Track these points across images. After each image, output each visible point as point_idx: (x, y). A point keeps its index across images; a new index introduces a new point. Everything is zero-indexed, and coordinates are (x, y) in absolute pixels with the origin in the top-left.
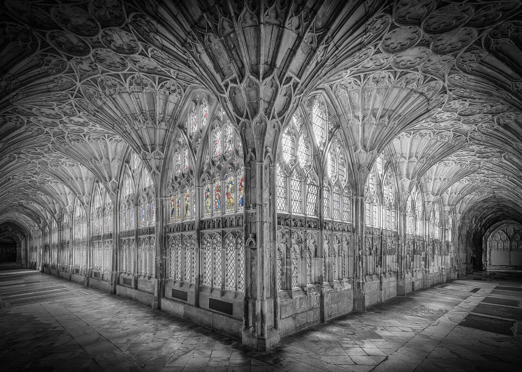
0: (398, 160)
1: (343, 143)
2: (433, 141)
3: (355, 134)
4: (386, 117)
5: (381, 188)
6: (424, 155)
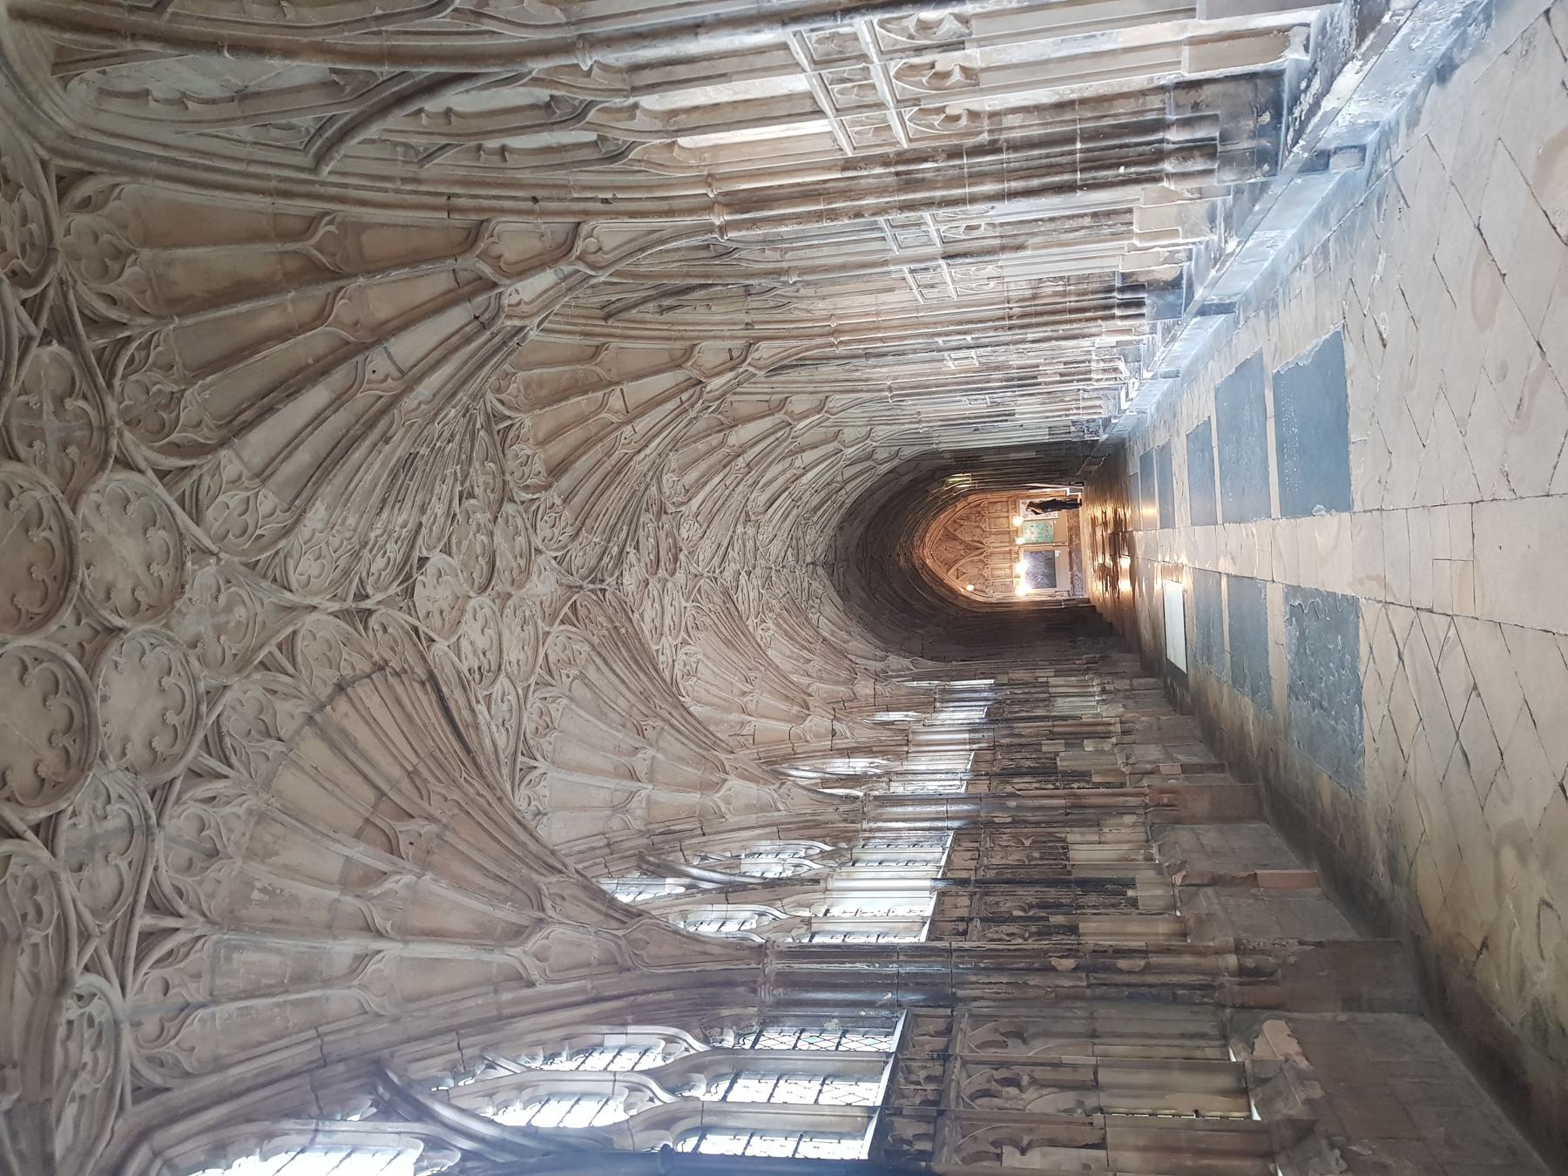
0: (638, 825)
2: (579, 689)
3: (439, 981)
4: (401, 826)
5: (744, 887)
6: (629, 725)
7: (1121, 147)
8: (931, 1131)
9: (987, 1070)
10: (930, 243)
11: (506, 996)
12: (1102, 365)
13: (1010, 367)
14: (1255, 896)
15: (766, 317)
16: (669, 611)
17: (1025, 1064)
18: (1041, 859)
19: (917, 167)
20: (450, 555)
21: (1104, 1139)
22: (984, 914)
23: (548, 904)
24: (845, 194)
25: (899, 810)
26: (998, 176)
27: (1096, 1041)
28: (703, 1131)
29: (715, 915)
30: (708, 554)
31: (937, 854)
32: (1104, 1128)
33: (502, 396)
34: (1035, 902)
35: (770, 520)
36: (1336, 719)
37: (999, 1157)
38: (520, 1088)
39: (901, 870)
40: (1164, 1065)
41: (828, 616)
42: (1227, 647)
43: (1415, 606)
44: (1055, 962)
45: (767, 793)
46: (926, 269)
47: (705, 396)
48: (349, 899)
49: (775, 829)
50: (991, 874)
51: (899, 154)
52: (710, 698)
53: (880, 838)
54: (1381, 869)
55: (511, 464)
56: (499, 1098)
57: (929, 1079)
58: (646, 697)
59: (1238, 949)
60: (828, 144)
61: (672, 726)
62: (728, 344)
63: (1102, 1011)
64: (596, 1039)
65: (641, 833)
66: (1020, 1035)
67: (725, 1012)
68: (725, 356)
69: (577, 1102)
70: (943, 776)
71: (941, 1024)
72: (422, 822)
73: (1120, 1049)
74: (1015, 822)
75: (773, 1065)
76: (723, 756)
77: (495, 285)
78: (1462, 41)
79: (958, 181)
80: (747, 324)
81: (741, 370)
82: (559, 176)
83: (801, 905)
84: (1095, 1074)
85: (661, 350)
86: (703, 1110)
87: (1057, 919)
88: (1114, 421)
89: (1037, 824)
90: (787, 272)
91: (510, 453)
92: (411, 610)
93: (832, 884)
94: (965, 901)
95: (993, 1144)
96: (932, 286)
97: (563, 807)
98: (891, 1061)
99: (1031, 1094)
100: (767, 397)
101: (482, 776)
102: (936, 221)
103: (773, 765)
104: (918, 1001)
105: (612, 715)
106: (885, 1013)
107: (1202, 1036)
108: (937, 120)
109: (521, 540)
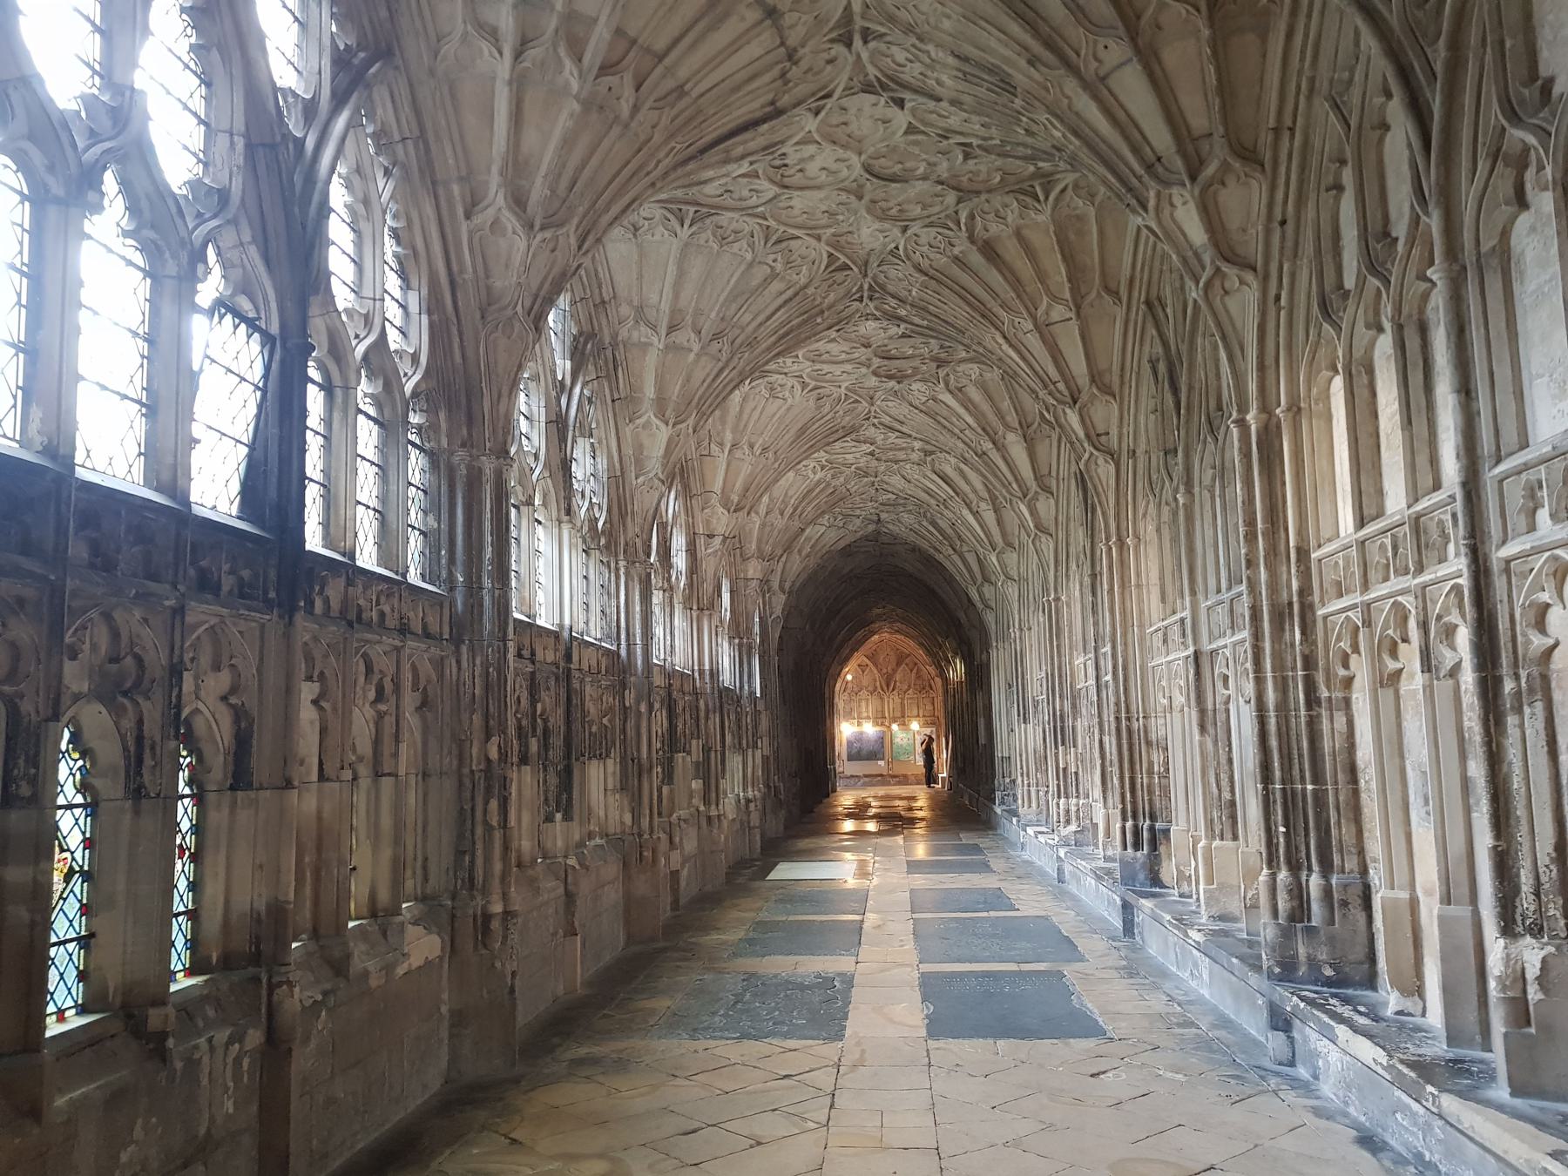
0: (623, 334)
1: (408, 153)
2: (760, 273)
4: (628, 78)
5: (563, 439)
7: (1306, 829)
8: (332, 614)
9: (392, 670)
10: (1211, 640)
11: (456, 189)
12: (1073, 809)
13: (1075, 719)
14: (555, 934)
15: (1140, 472)
16: (837, 370)
17: (397, 707)
18: (590, 733)
19: (1296, 624)
20: (906, 133)
21: (328, 780)
22: (538, 675)
23: (548, 234)
24: (1273, 552)
25: (637, 598)
26: (1283, 707)
27: (420, 777)
28: (327, 388)
29: (535, 409)
30: (893, 412)
31: (594, 634)
32: (338, 780)
33: (1070, 190)
34: (550, 725)
35: (925, 476)
36: (725, 1016)
37: (309, 678)
38: (366, 202)
39: (579, 598)
40: (397, 840)
41: (825, 534)
42: (791, 918)
43: (837, 1093)
44: (495, 740)
45: (654, 465)
46: (1184, 635)
47: (1060, 407)
48: (553, 23)
49: (618, 474)
50: (576, 684)
51: (1311, 607)
52: (747, 411)
53: (609, 578)
54: (583, 1051)
55: (997, 200)
56: (356, 180)
57: (382, 614)
58: (751, 343)
59: (508, 914)
60: (1325, 533)
61: (721, 371)
62: (1114, 432)
63: (449, 785)
64: (414, 282)
65: (615, 336)
66: (424, 705)
67: (442, 415)
68: (1101, 429)
69: (354, 261)
70: (668, 643)
71: (434, 628)
72: (631, 101)
73: (412, 799)
74: (625, 710)
75: (392, 460)
76: (691, 421)
77: (1193, 178)
78: (1400, 1161)
79: (1279, 666)
80: (1134, 452)
81: (1086, 445)
82: (1308, 248)
83: (545, 496)
84: (389, 774)
85: (1111, 357)
86: (349, 389)
87: (534, 745)
88: (1014, 820)
89: (624, 731)
90: (1189, 491)
91: (1009, 199)
92: (849, 91)
94: (550, 658)
95: (322, 674)
96: (1165, 641)
97: (642, 255)
98: (399, 578)
99: (370, 712)
100: (1054, 473)
101: (675, 168)
102: (1235, 644)
103: (681, 474)
104: (456, 606)
105: (734, 307)
106: (444, 574)
107: (426, 879)
108: (1345, 645)
109: (917, 211)
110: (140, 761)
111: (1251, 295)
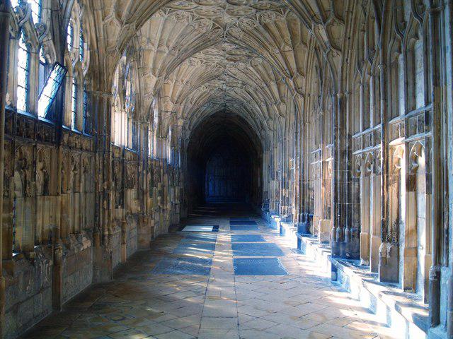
0: (143, 46)
9: (78, 161)
15: (311, 101)
24: (342, 134)
26: (342, 180)
44: (106, 183)
45: (151, 90)
51: (351, 151)
55: (269, 12)
58: (186, 50)
60: (356, 130)
62: (304, 88)
63: (92, 196)
67: (92, 81)
77: (325, 23)
82: (355, 47)
85: (303, 65)
89: (138, 180)
90: (324, 111)
91: (272, 12)
93: (123, 113)
103: (158, 93)
108: (359, 163)
109: (243, 13)
110: (26, 187)
111: (340, 58)
